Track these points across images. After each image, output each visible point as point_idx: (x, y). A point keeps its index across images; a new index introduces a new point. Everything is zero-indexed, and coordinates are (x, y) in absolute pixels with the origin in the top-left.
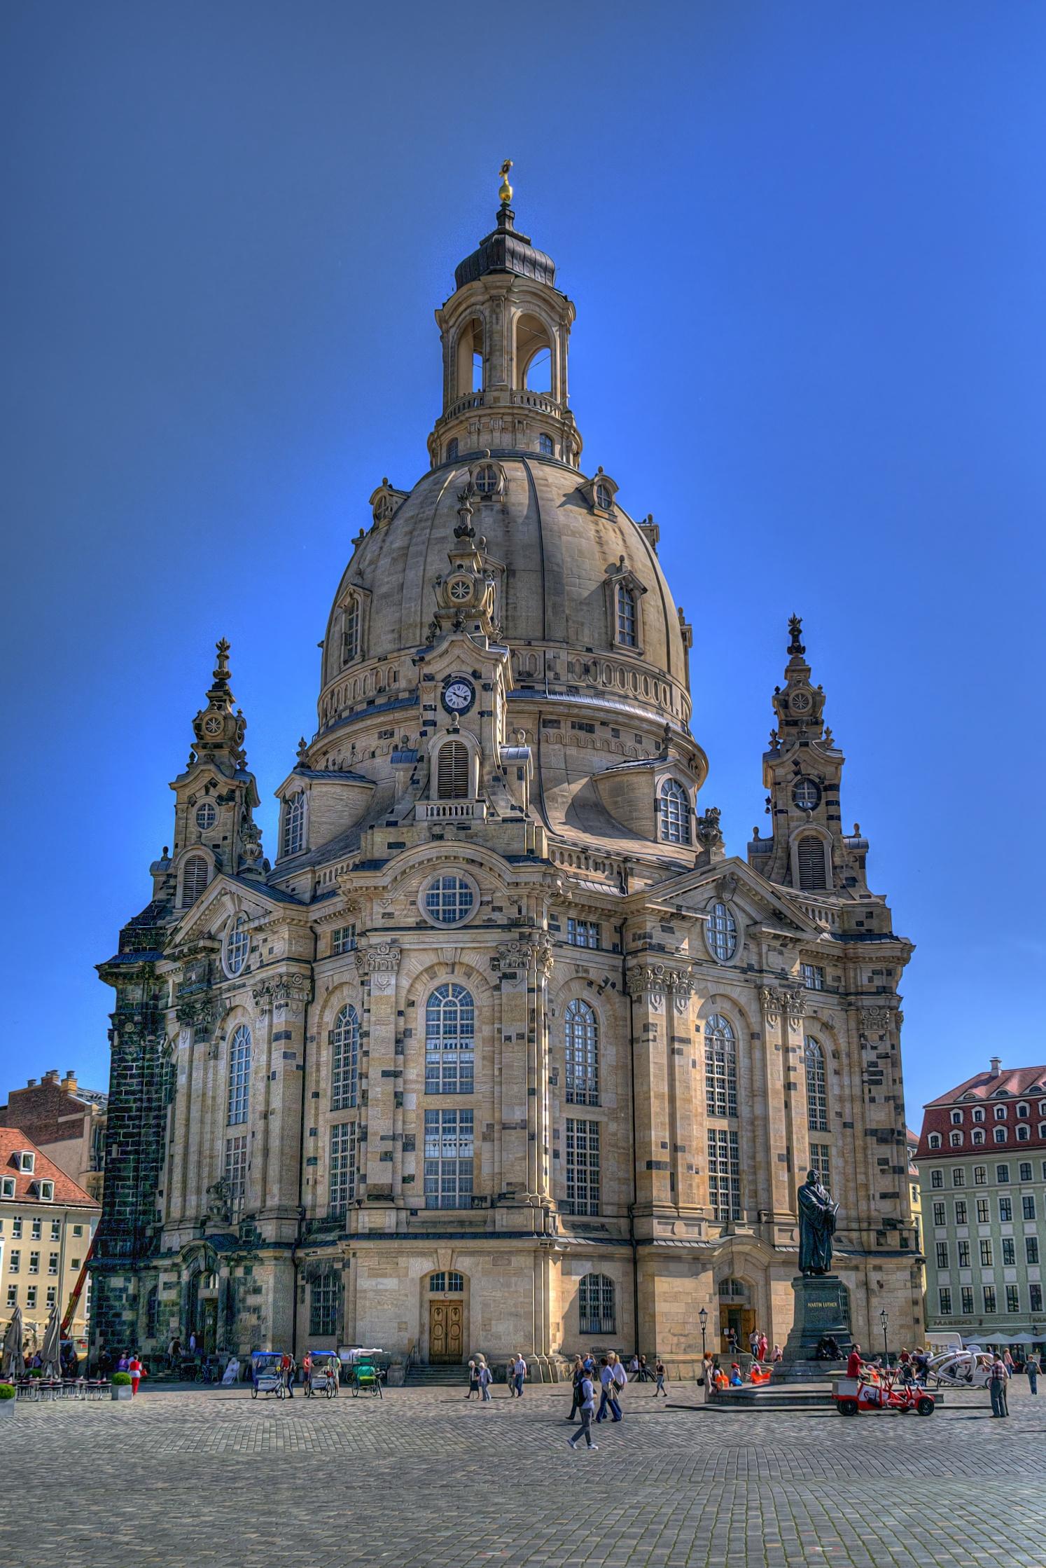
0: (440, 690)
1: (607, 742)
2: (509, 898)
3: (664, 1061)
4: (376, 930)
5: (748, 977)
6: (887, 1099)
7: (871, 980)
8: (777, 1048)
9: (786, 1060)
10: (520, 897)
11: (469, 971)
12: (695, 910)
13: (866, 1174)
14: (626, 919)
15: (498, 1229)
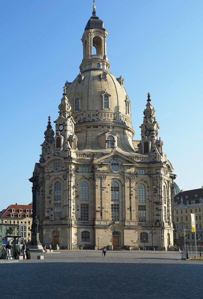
0: (58, 127)
1: (101, 129)
2: (65, 165)
3: (100, 192)
4: (46, 173)
5: (121, 174)
6: (158, 196)
7: (155, 171)
8: (128, 187)
9: (131, 189)
10: (67, 165)
11: (60, 179)
12: (106, 163)
13: (154, 211)
14: (93, 166)
15: (63, 223)
